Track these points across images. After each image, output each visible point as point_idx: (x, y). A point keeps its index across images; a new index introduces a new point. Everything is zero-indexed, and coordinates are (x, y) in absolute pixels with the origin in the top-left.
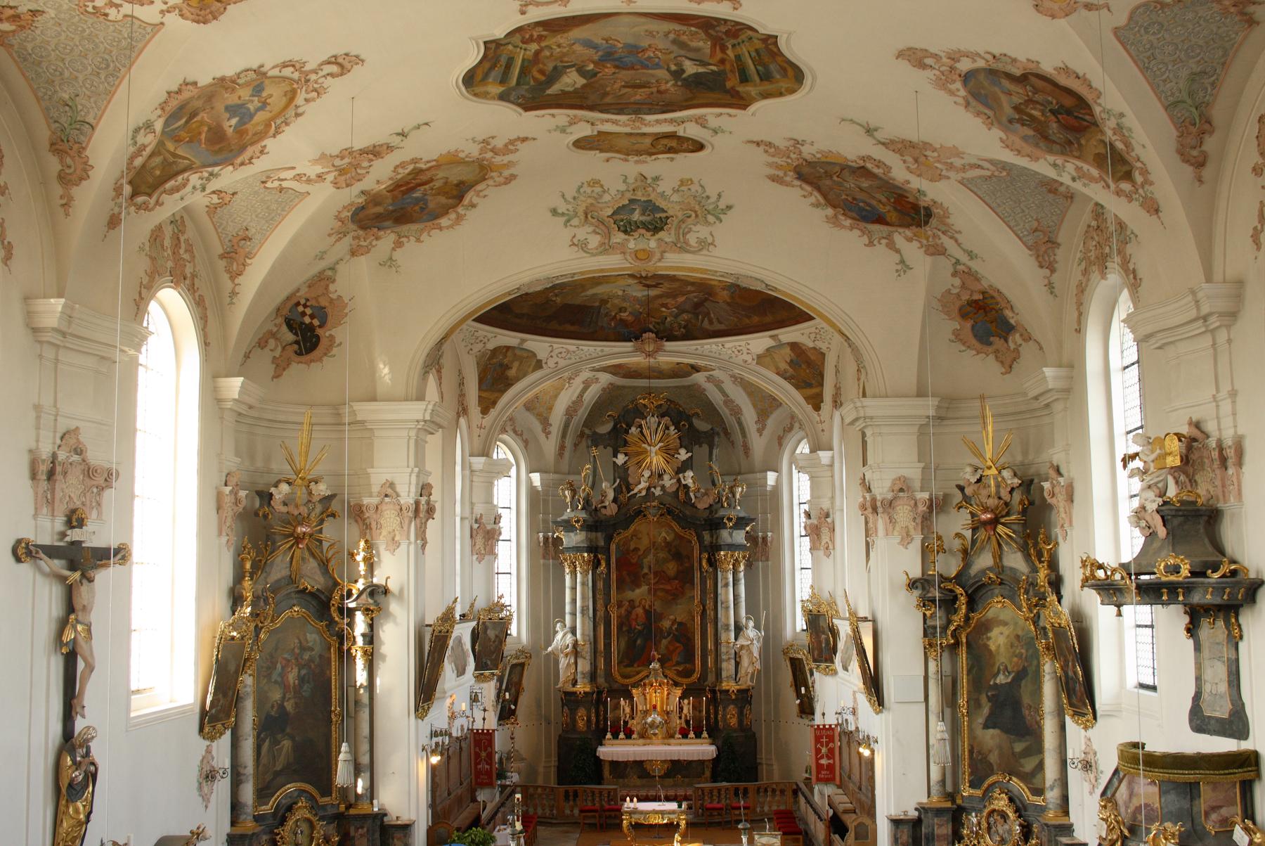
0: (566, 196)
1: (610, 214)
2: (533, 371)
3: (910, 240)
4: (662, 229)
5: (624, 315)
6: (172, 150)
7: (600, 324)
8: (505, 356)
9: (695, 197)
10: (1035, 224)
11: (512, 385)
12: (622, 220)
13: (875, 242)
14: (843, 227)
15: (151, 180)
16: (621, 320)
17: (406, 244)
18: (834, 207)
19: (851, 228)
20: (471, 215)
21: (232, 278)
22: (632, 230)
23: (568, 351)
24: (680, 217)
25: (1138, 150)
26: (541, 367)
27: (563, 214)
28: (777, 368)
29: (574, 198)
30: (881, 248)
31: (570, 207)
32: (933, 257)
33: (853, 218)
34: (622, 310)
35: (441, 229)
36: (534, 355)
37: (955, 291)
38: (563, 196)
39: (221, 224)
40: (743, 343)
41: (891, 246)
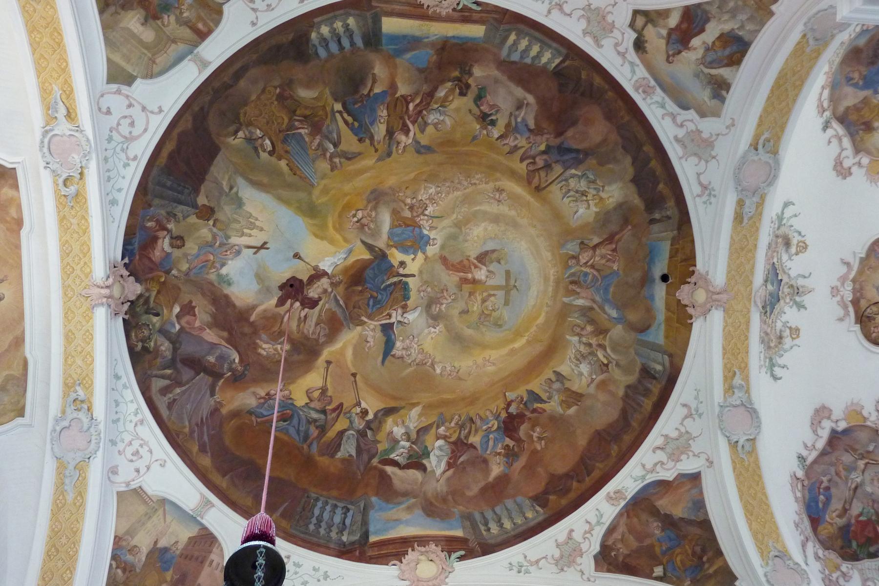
2: (109, 60)
3: (817, 557)
5: (165, 244)
7: (156, 201)
8: (183, 22)
11: (101, 12)
14: (794, 493)
16: (155, 239)
18: (807, 474)
23: (130, 139)
26: (112, 78)
28: (131, 533)
33: (804, 497)
34: (178, 241)
36: (150, 75)
40: (159, 454)
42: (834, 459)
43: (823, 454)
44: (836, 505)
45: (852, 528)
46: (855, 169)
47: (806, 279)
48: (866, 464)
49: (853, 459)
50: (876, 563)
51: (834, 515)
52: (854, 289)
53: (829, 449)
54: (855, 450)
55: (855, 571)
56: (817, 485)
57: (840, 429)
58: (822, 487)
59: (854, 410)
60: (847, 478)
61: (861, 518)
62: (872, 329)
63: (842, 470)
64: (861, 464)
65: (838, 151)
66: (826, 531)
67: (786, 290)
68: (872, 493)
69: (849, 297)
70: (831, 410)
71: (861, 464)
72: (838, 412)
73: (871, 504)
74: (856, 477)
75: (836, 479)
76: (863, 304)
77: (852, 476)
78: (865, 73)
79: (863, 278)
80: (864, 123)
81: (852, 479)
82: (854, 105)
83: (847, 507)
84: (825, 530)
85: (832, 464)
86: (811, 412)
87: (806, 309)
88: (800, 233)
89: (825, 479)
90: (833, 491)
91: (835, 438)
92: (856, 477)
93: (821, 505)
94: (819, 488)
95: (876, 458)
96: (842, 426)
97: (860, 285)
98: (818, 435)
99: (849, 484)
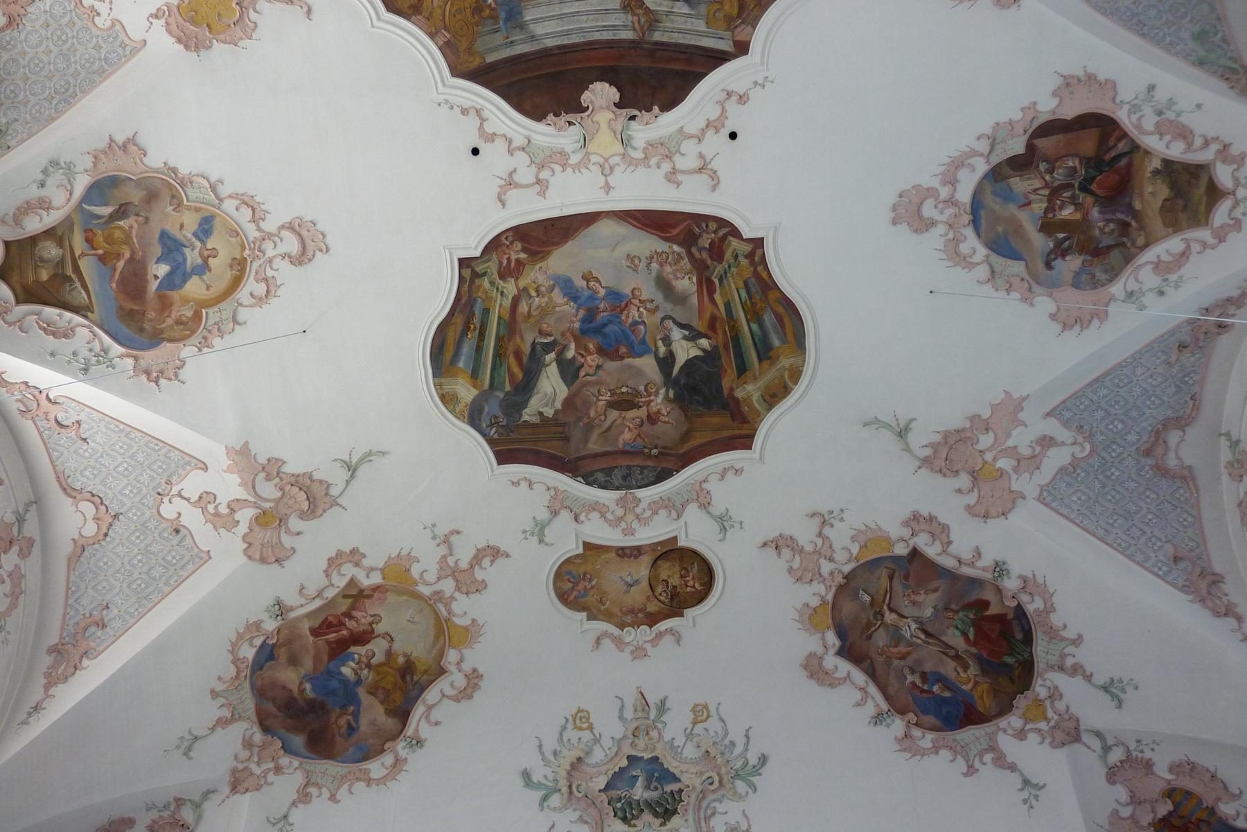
0: (544, 749)
1: (602, 787)
3: (1021, 735)
4: (675, 812)
6: (77, 253)
9: (715, 743)
10: (1170, 549)
12: (619, 800)
13: (977, 765)
14: (923, 753)
15: (30, 277)
17: (314, 800)
18: (902, 712)
19: (936, 750)
20: (416, 760)
21: (47, 687)
22: (634, 817)
24: (699, 788)
25: (1200, 125)
27: (539, 786)
29: (555, 753)
30: (988, 772)
31: (548, 771)
32: (1065, 749)
35: (369, 782)
37: (1126, 812)
38: (540, 746)
39: (78, 587)
41: (1001, 761)
42: (881, 659)
43: (872, 674)
44: (949, 669)
45: (985, 655)
46: (467, 667)
47: (625, 704)
48: (891, 610)
49: (881, 630)
50: (1039, 638)
51: (962, 674)
52: (632, 625)
53: (866, 664)
54: (869, 625)
55: (1046, 676)
56: (917, 692)
57: (838, 643)
58: (920, 685)
59: (810, 618)
60: (911, 644)
61: (971, 636)
62: (689, 589)
63: (896, 650)
64: (890, 617)
65: (445, 700)
66: (985, 696)
67: (641, 743)
68: (935, 608)
69: (645, 633)
70: (810, 655)
71: (890, 617)
72: (812, 643)
73: (950, 614)
74: (909, 629)
75: (909, 661)
76: (653, 607)
77: (908, 635)
78: (338, 710)
79: (616, 610)
80: (403, 677)
81: (912, 636)
82: (382, 703)
83: (952, 653)
84: (984, 702)
85: (888, 662)
86: (812, 684)
87: (666, 698)
88: (564, 728)
89: (910, 678)
90: (927, 668)
91: (849, 652)
92: (909, 629)
93: (947, 694)
94: (923, 691)
95: (883, 592)
96: (832, 638)
97: (626, 614)
98: (845, 679)
99: (919, 641)
